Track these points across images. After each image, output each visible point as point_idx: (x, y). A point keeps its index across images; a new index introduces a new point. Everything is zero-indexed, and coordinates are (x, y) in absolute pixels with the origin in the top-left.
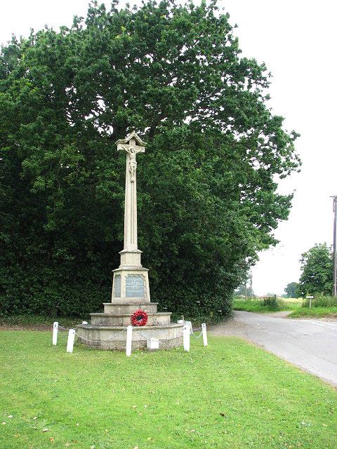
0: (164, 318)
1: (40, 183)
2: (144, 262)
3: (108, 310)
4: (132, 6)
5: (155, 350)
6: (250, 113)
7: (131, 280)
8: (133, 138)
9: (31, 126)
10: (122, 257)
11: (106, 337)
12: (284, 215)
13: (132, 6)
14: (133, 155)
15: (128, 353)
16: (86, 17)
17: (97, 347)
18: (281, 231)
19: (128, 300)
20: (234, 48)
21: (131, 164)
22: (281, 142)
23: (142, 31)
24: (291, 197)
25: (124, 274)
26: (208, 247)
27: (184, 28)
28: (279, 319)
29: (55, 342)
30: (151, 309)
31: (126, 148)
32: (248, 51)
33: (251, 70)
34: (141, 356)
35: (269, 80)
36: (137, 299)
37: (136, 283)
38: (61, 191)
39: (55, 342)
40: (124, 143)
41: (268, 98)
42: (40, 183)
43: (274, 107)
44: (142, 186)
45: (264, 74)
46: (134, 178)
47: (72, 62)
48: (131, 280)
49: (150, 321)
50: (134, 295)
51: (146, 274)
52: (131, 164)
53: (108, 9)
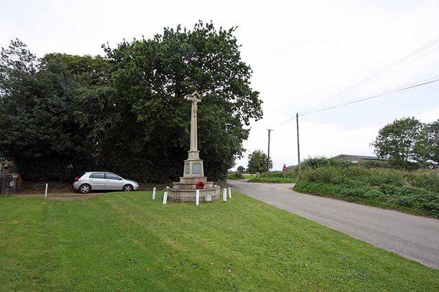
0: (211, 185)
1: (140, 118)
2: (201, 157)
3: (182, 181)
4: (187, 31)
5: (209, 202)
6: (240, 88)
7: (194, 165)
8: (196, 94)
9: (137, 88)
10: (189, 154)
11: (184, 195)
12: (246, 138)
13: (187, 31)
14: (196, 103)
15: (197, 204)
16: (163, 35)
17: (178, 201)
18: (245, 144)
19: (193, 175)
20: (237, 57)
21: (194, 107)
22: (256, 104)
23: (195, 44)
24: (249, 130)
25: (191, 163)
26: (221, 151)
27: (216, 42)
28: (381, 171)
29: (154, 198)
30: (204, 180)
31: (191, 99)
32: (245, 58)
33: (244, 69)
34: (204, 206)
35: (251, 74)
36: (197, 175)
37: (197, 167)
38: (153, 122)
39: (154, 198)
40: (191, 96)
41: (250, 83)
42: (140, 118)
43: (253, 87)
44: (199, 116)
45: (249, 71)
46: (196, 115)
47: (160, 55)
48: (194, 165)
49: (205, 187)
50: (196, 173)
51: (202, 163)
52: (194, 107)
53: (175, 31)
